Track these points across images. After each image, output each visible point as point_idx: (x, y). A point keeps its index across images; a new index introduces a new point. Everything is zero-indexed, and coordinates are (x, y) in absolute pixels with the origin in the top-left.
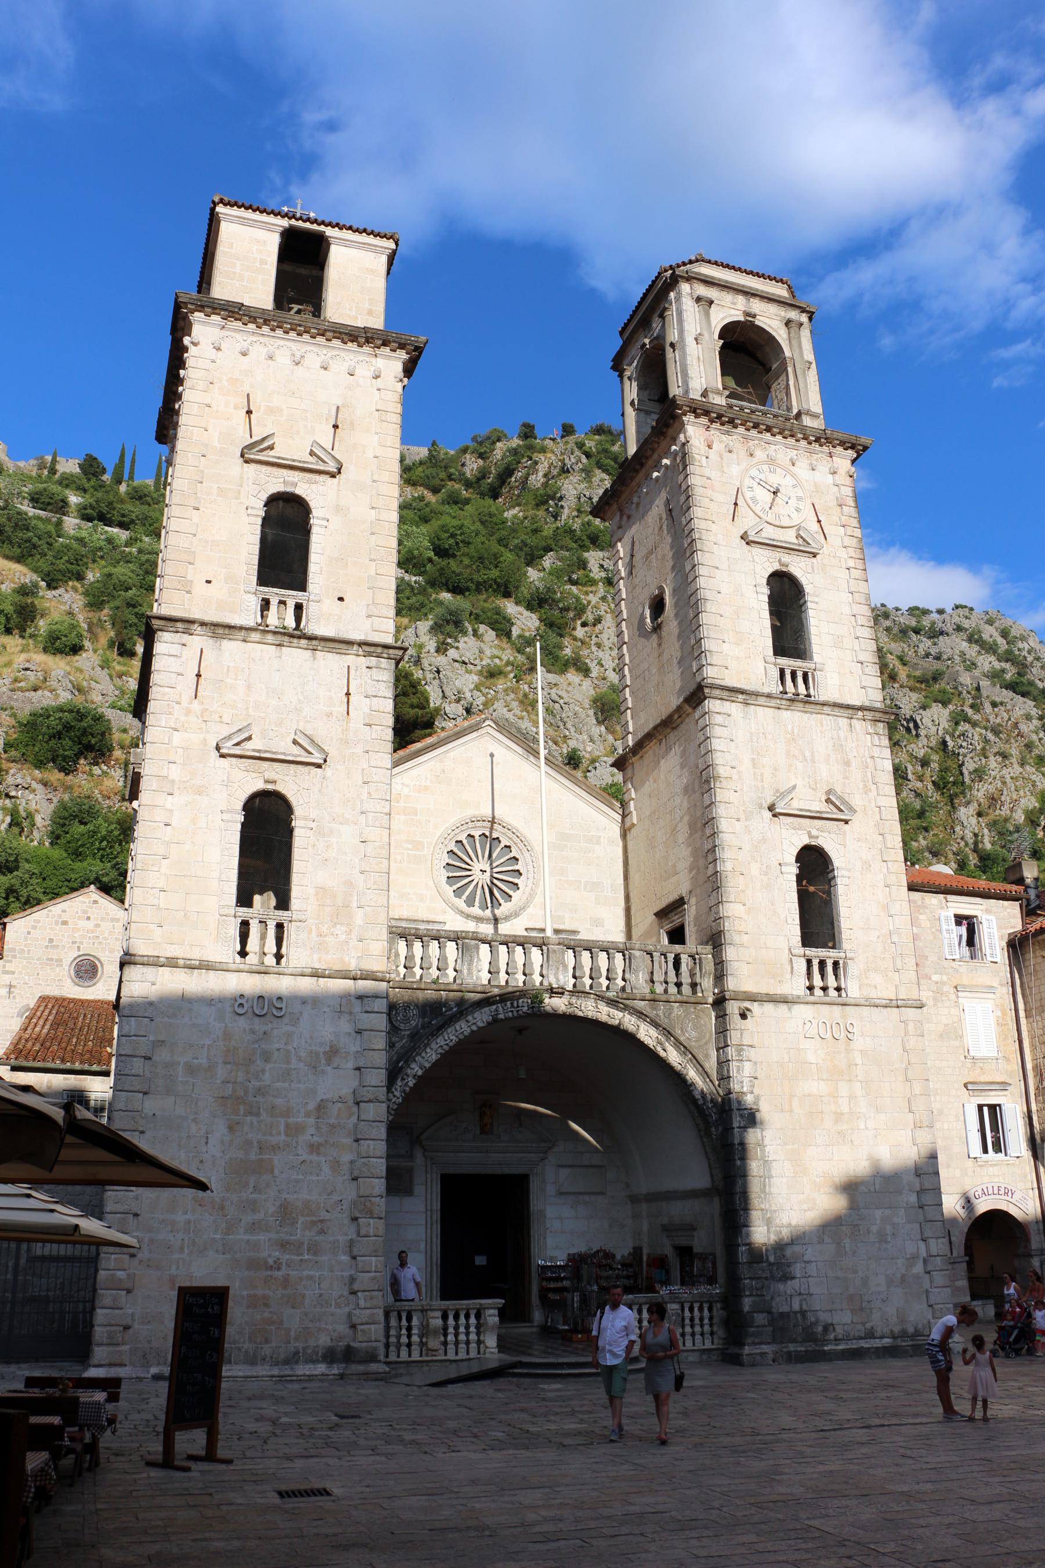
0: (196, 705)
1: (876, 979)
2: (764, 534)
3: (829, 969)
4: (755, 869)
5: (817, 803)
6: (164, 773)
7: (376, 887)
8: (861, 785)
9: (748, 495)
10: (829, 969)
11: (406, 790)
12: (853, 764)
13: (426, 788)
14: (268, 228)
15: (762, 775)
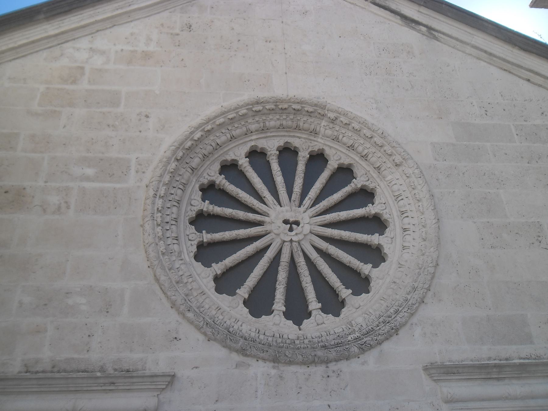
13: (147, 56)
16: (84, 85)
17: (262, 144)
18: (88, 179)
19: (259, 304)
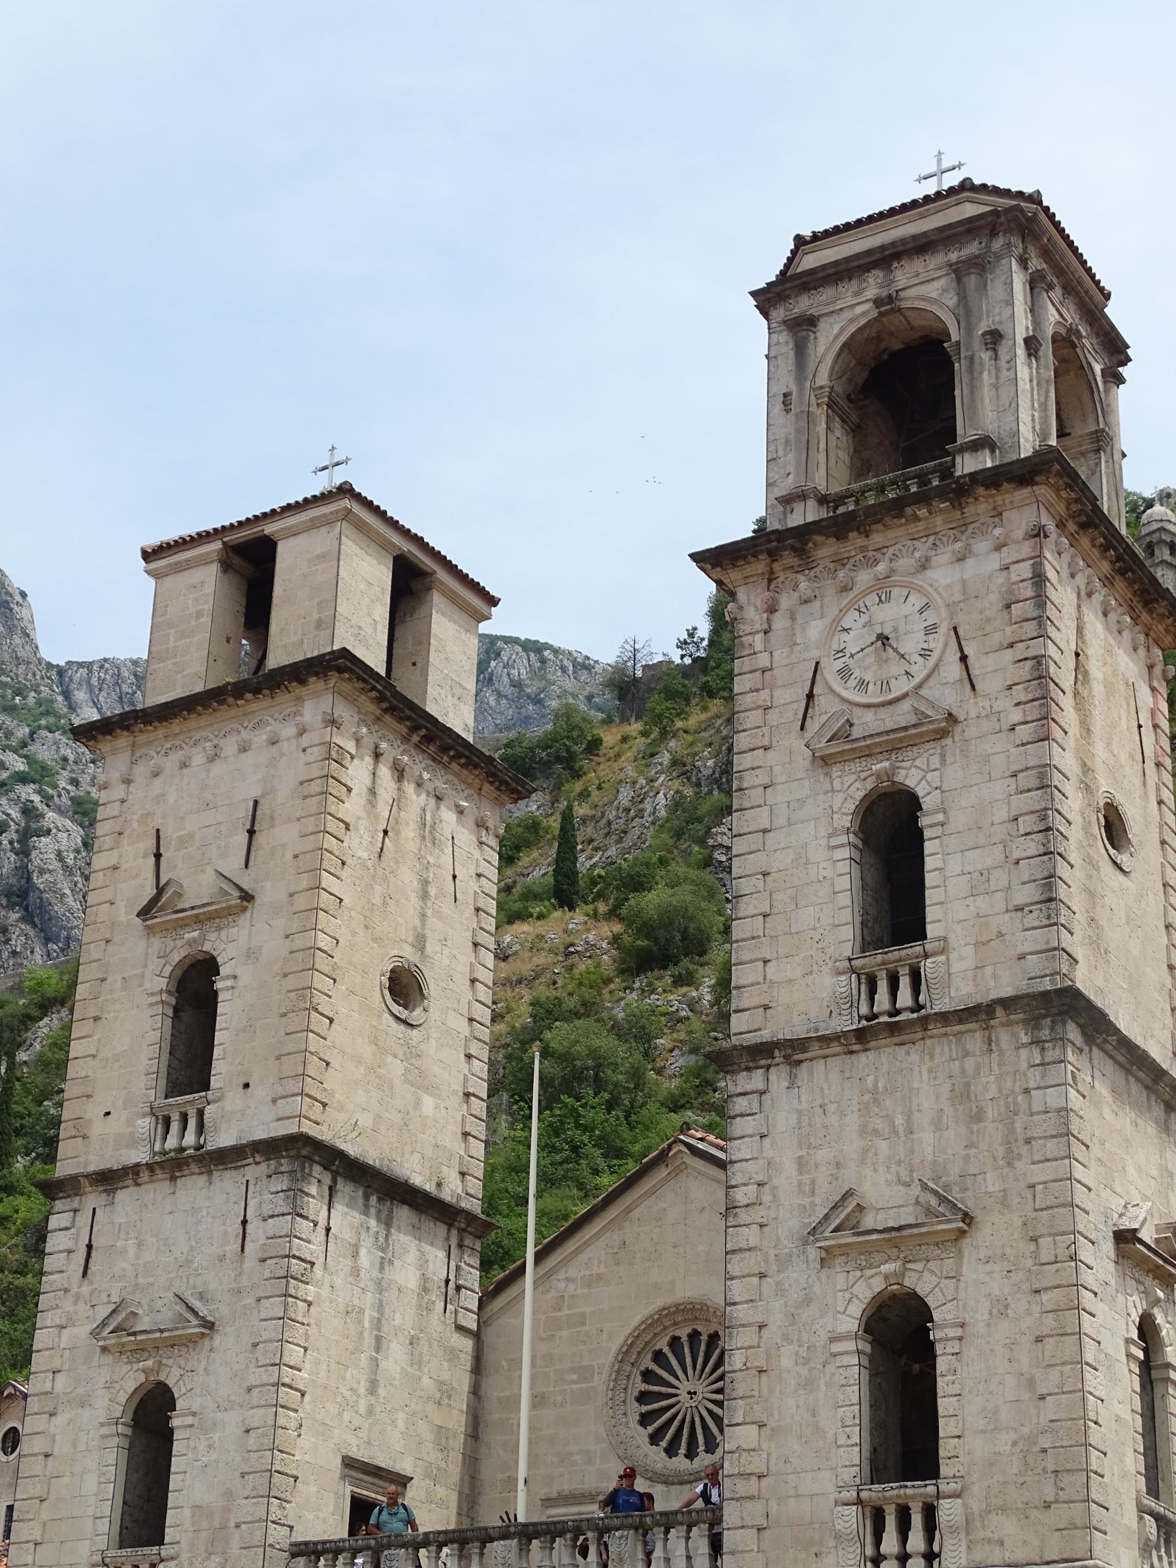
0: (85, 1289)
1: (1007, 1527)
2: (856, 733)
3: (917, 1520)
4: (787, 1359)
5: (911, 1208)
7: (254, 1493)
8: (1001, 1153)
9: (830, 671)
10: (917, 1520)
11: (571, 1288)
12: (990, 1113)
13: (599, 1277)
14: (203, 562)
15: (813, 1182)
16: (566, 1311)
17: (677, 1333)
18: (574, 1382)
19: (671, 1451)
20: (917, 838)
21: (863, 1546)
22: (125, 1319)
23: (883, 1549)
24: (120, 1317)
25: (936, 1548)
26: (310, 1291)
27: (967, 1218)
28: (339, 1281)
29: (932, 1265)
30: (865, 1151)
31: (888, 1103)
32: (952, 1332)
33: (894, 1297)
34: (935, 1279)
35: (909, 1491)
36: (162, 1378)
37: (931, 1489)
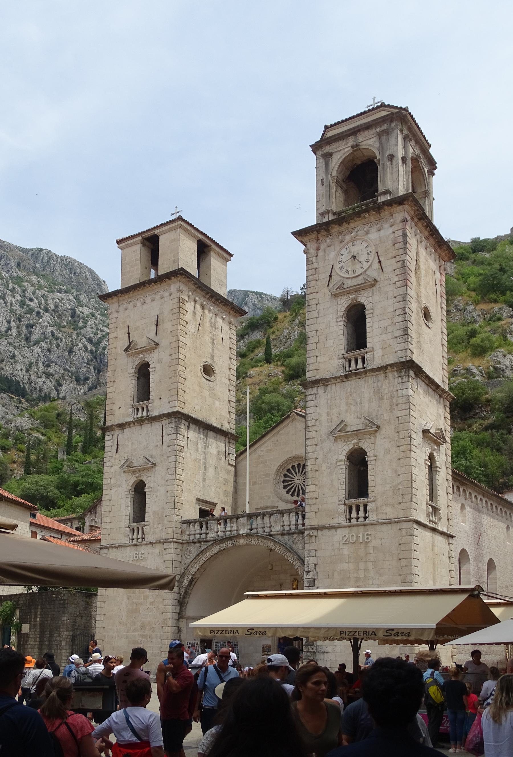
2: (345, 286)
3: (362, 508)
6: (109, 482)
10: (362, 508)
20: (364, 318)
21: (346, 516)
22: (130, 463)
23: (352, 516)
24: (128, 463)
25: (367, 515)
26: (184, 454)
27: (378, 427)
28: (192, 452)
29: (367, 440)
30: (347, 410)
31: (354, 395)
32: (372, 458)
33: (356, 449)
34: (368, 444)
35: (359, 501)
36: (141, 479)
37: (366, 500)
